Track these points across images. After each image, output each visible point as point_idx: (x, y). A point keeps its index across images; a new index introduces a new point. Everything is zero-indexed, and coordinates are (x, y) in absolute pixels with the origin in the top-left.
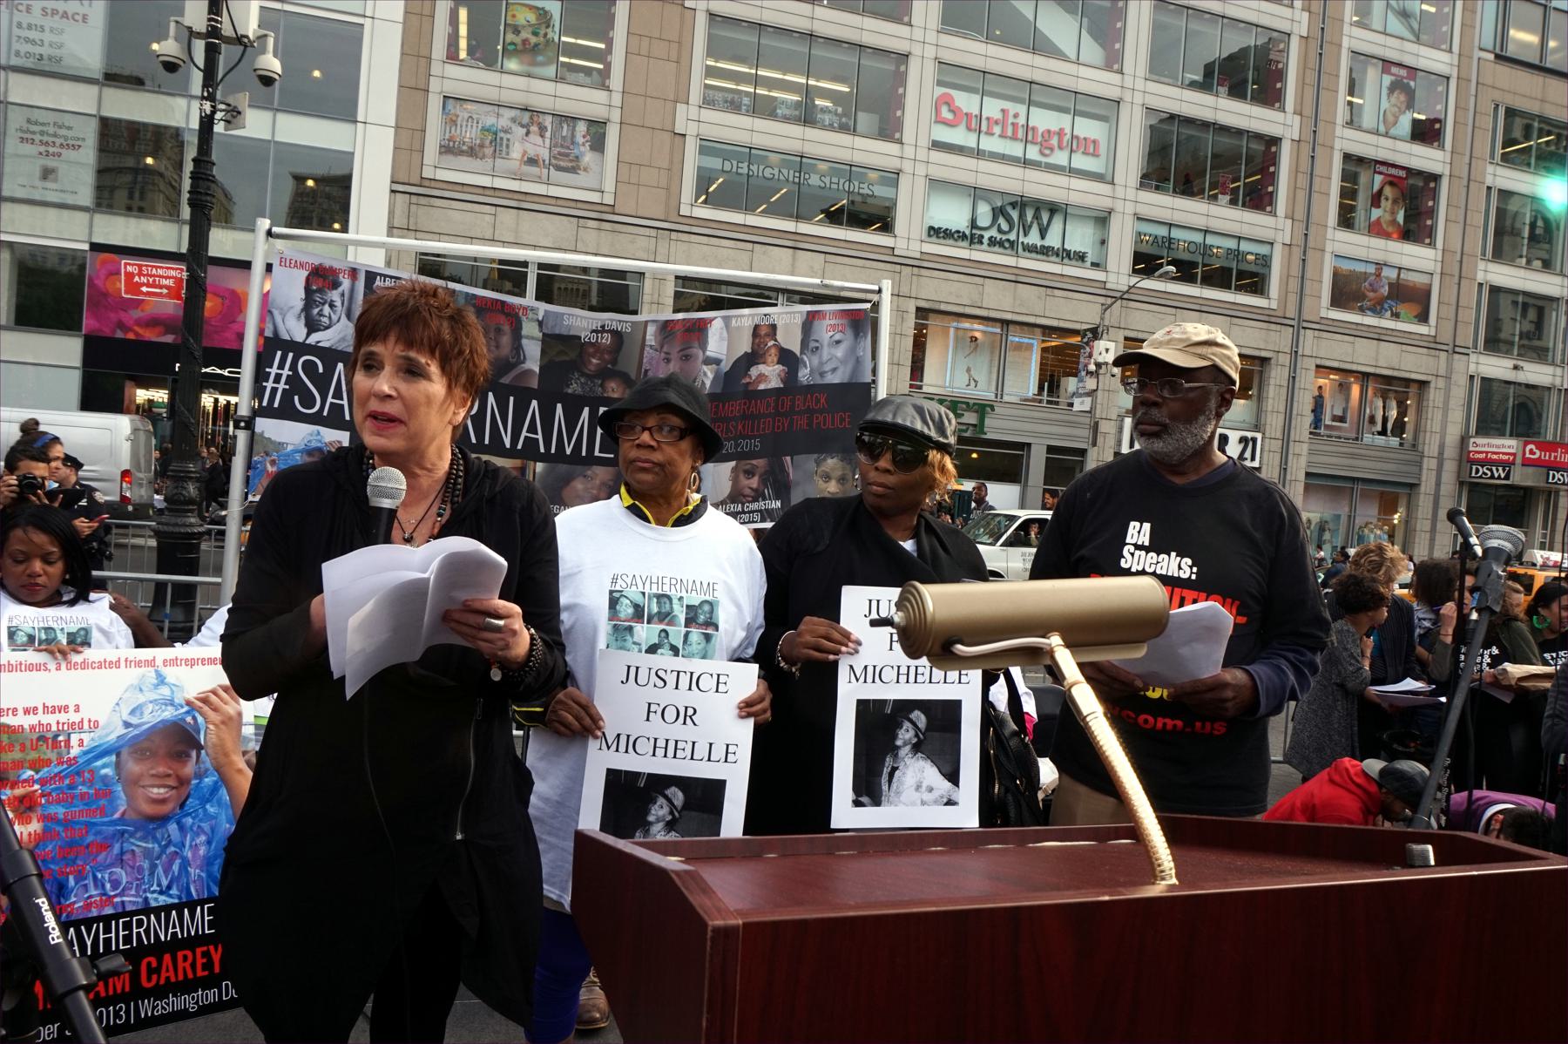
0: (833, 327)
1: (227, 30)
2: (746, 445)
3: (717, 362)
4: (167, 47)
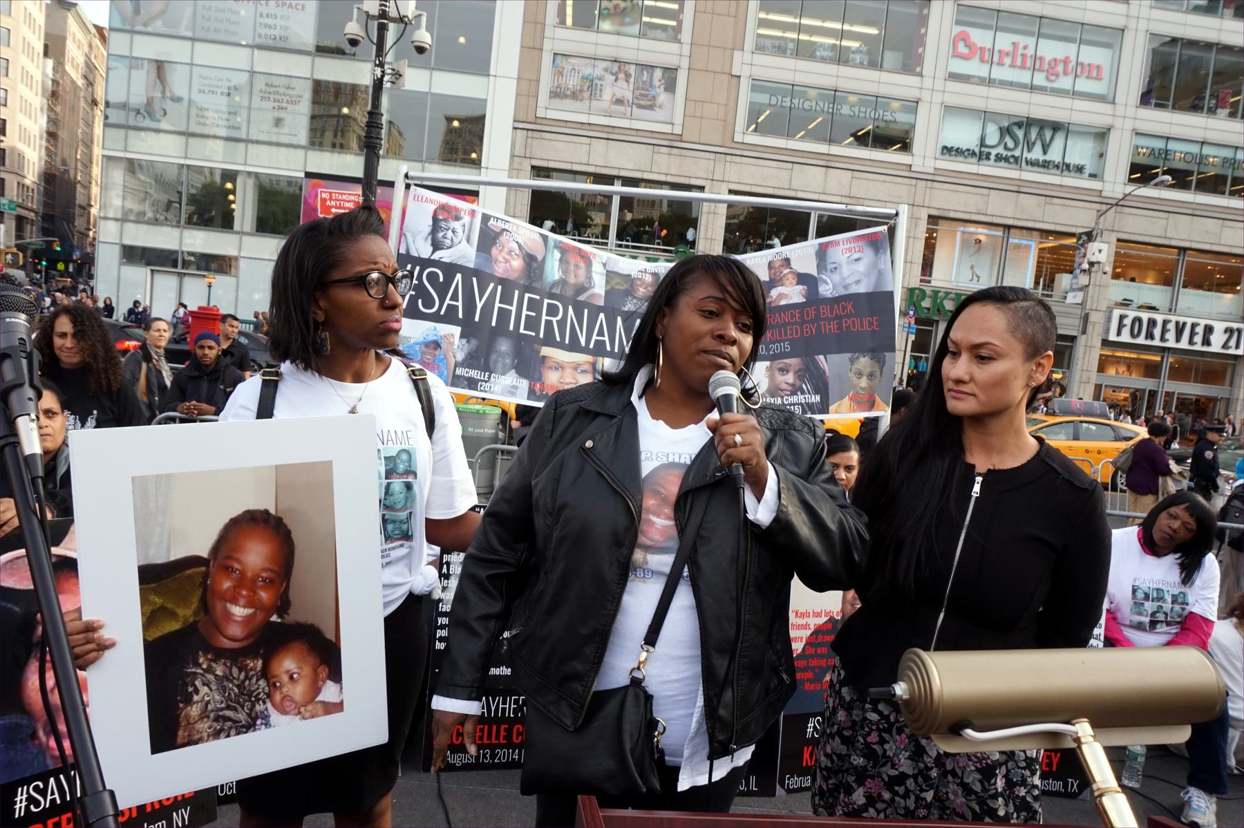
1: (393, 12)
4: (353, 28)
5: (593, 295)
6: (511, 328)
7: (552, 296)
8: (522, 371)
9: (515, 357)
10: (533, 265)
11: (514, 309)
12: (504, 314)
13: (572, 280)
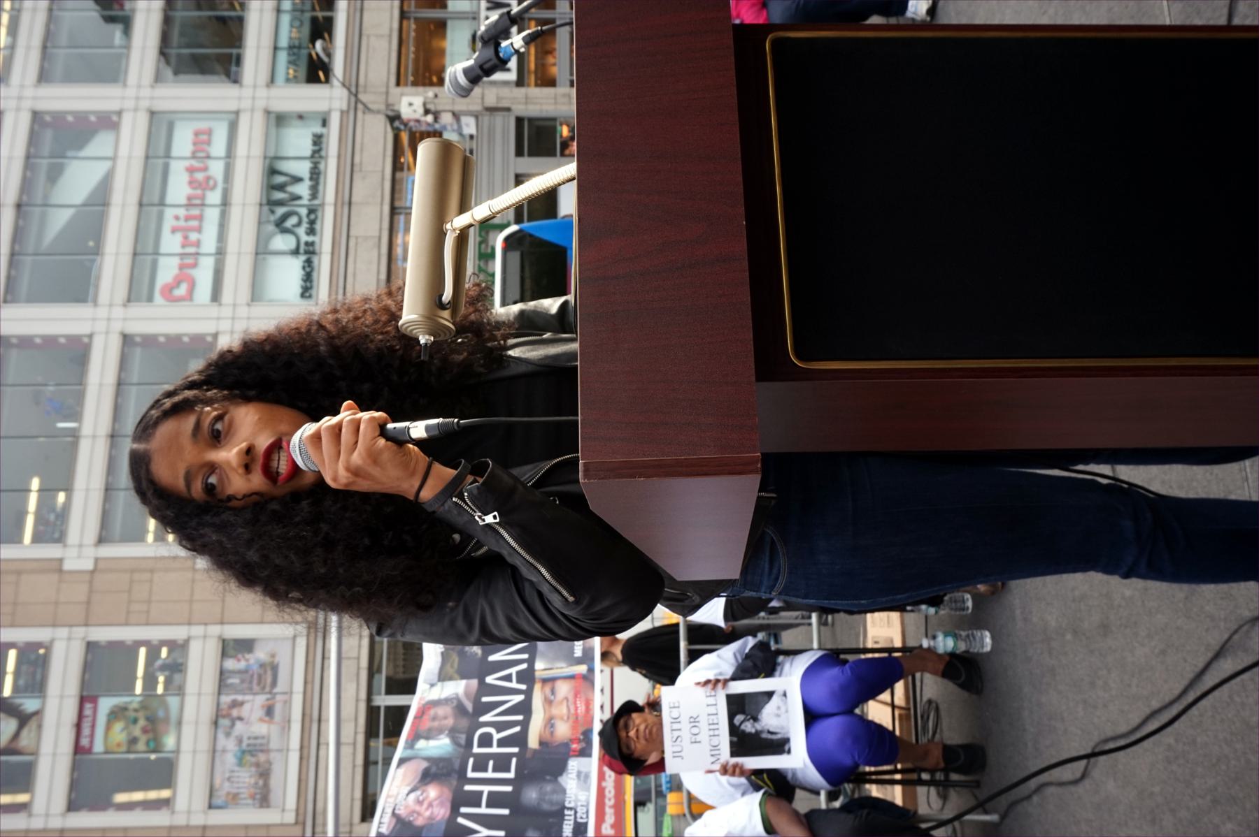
5: (467, 694)
6: (509, 789)
7: (469, 744)
8: (561, 768)
9: (544, 780)
10: (434, 772)
11: (486, 789)
12: (495, 800)
13: (450, 722)
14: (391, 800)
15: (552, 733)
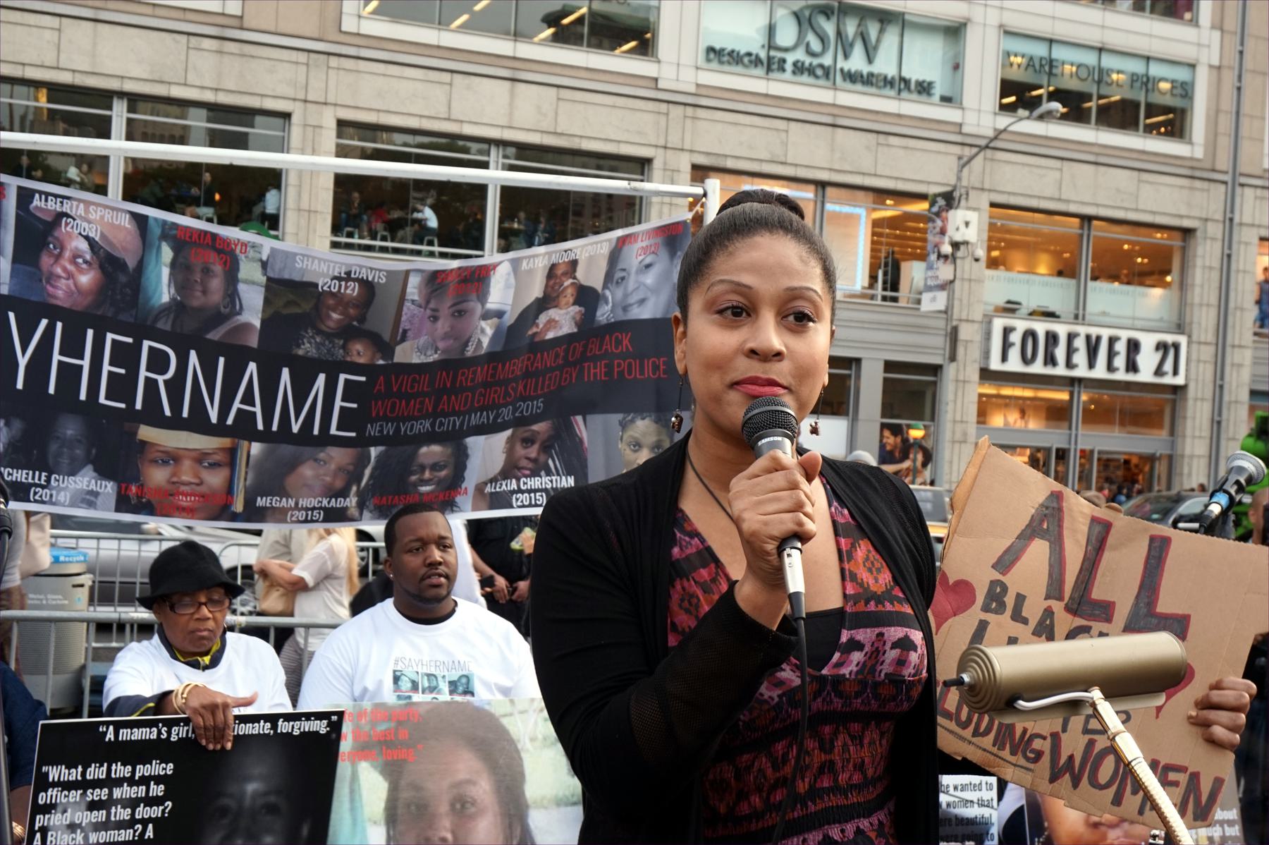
0: (645, 249)
2: (528, 408)
3: (500, 314)
6: (83, 397)
11: (86, 363)
12: (69, 375)
14: (81, 210)
15: (154, 461)
